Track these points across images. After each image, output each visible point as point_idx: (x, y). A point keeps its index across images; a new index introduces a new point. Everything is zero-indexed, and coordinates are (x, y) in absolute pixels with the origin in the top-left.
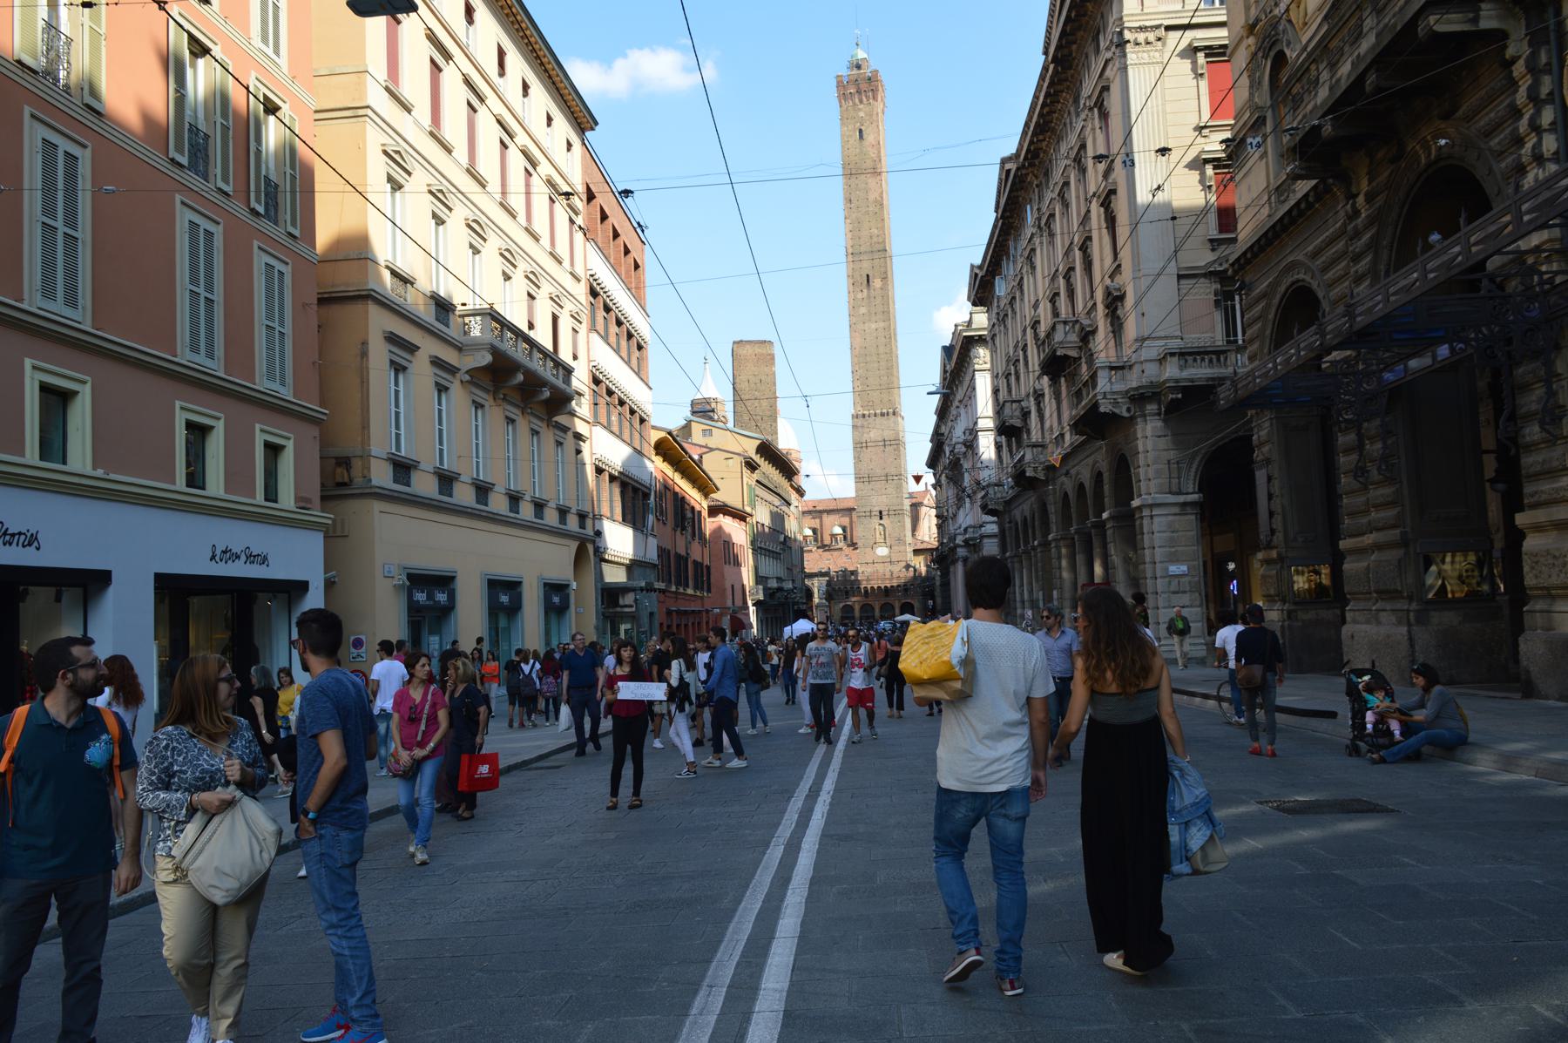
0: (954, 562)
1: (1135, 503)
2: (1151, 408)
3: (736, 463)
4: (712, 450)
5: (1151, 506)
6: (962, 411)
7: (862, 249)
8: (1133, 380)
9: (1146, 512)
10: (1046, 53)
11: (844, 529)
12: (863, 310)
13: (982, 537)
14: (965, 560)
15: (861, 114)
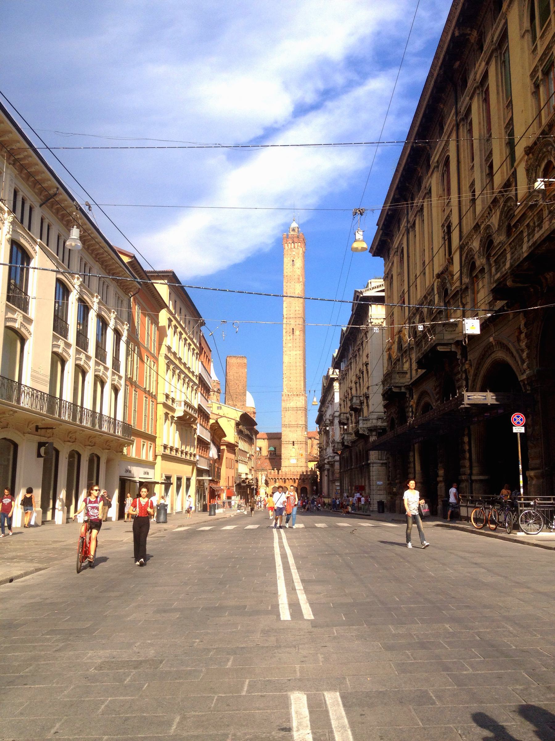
0: (324, 470)
1: (369, 462)
2: (374, 433)
3: (233, 423)
4: (222, 417)
5: (373, 463)
6: (330, 406)
7: (291, 316)
8: (369, 424)
9: (371, 465)
10: (352, 311)
11: (275, 449)
12: (290, 345)
13: (334, 461)
14: (328, 470)
15: (294, 253)
